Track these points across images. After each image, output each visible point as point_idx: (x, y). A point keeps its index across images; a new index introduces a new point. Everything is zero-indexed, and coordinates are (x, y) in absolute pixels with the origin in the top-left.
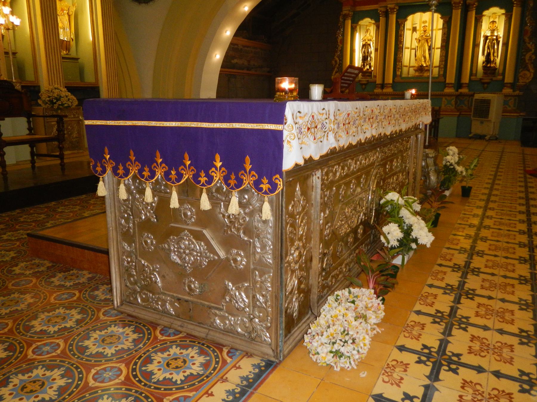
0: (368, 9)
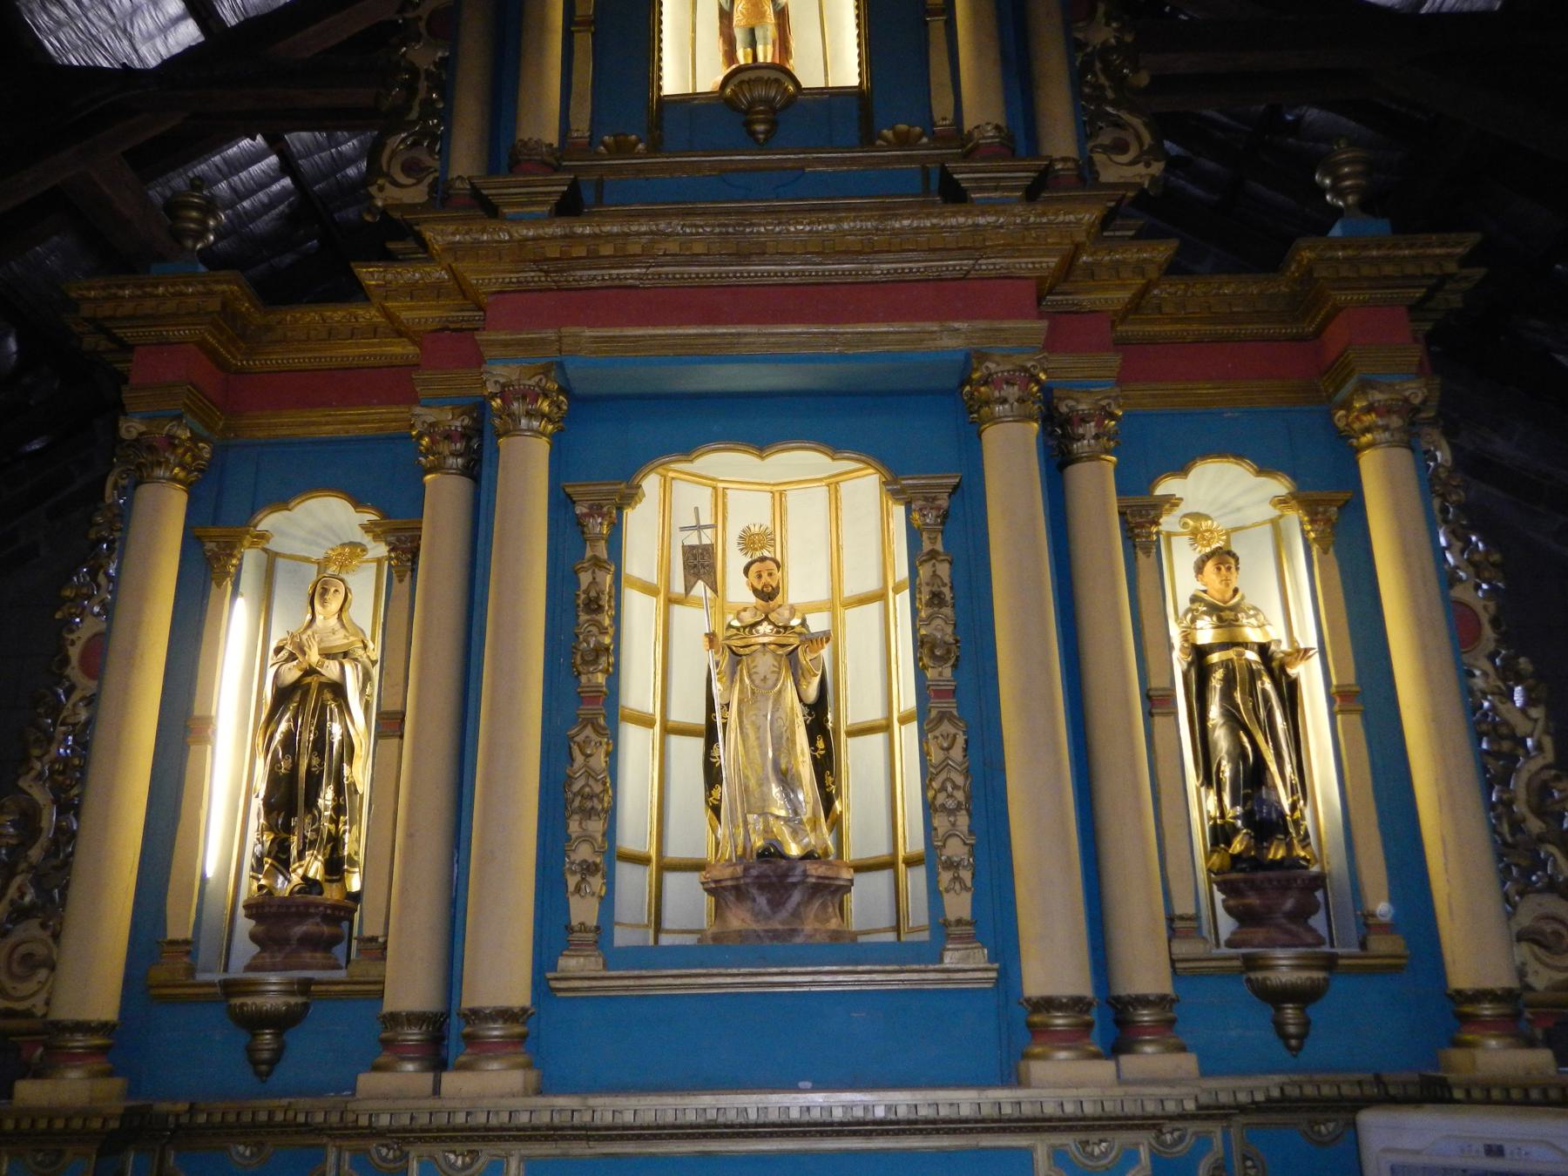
0: (327, 431)
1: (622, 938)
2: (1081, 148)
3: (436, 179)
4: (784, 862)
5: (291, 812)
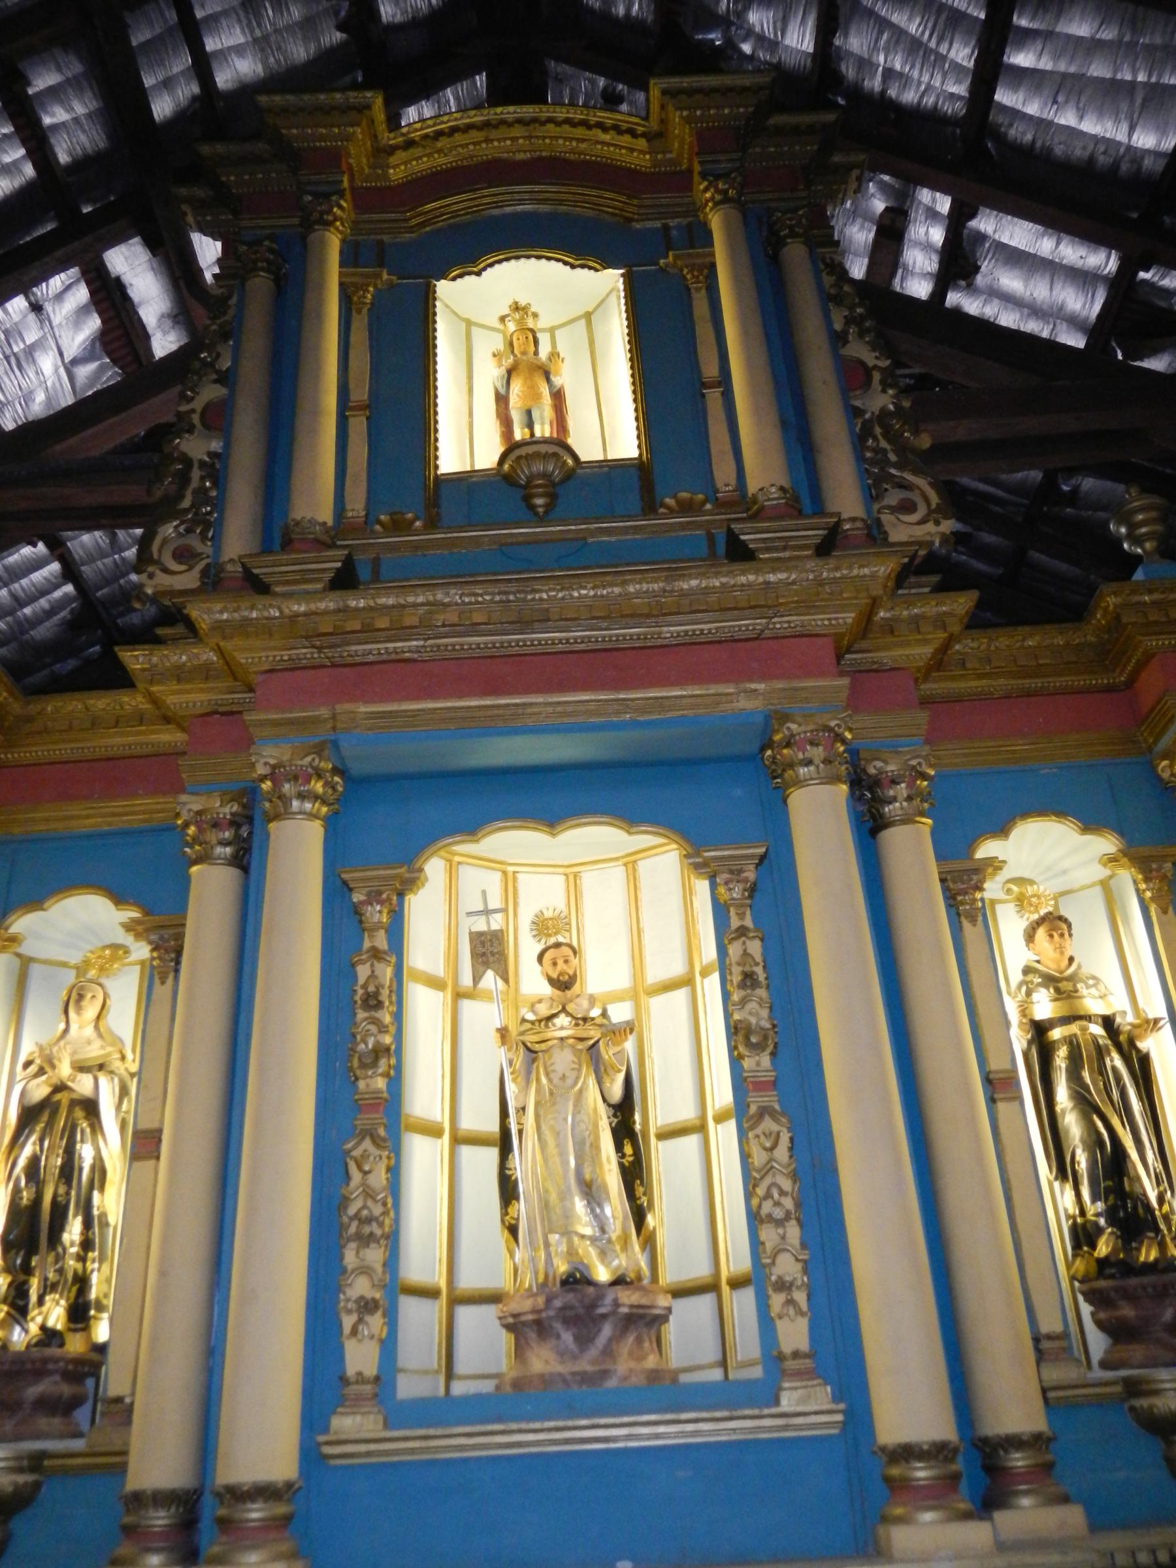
0: (86, 825)
1: (407, 1388)
2: (869, 511)
3: (208, 565)
4: (591, 1289)
5: (31, 1248)
